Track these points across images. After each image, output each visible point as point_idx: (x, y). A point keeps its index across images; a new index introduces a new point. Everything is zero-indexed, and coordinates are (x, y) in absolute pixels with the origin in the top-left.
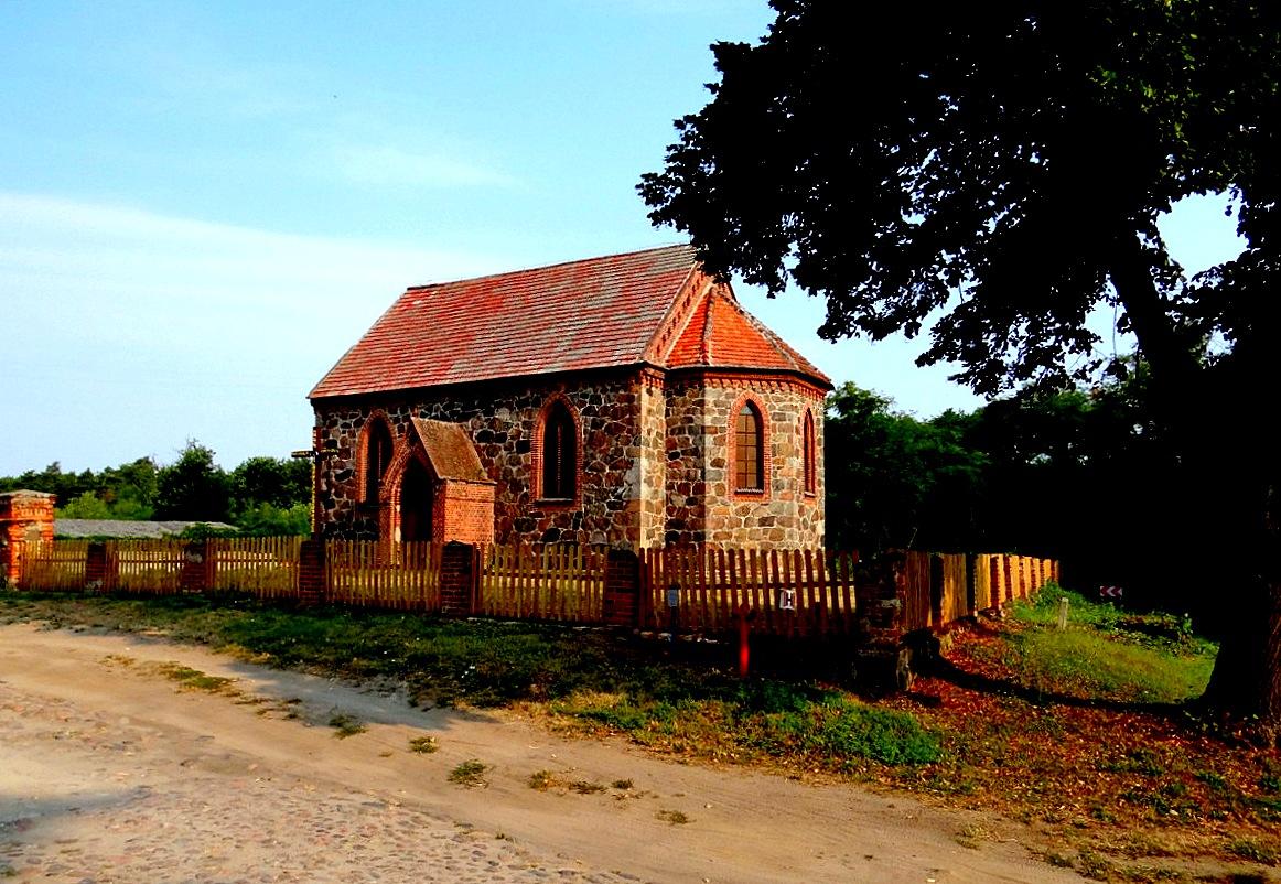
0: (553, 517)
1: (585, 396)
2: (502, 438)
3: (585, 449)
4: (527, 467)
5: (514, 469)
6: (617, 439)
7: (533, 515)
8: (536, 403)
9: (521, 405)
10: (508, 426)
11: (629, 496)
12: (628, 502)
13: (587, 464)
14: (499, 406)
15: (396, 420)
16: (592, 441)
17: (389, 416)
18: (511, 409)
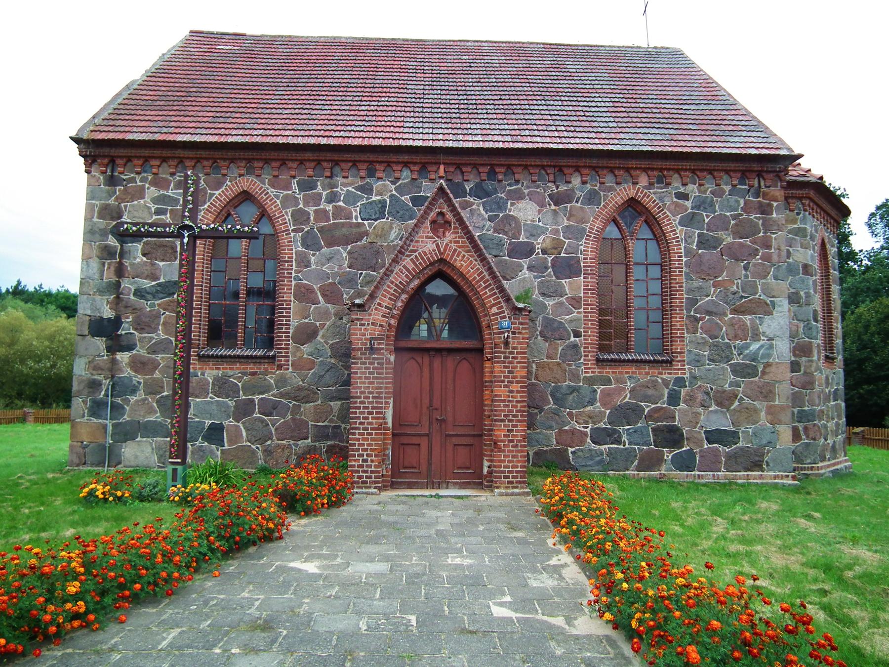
0: (629, 385)
1: (685, 197)
2: (527, 250)
3: (689, 278)
4: (575, 302)
5: (550, 303)
6: (746, 268)
7: (590, 381)
8: (592, 198)
9: (558, 200)
10: (535, 232)
11: (769, 356)
12: (768, 365)
13: (692, 302)
14: (518, 196)
15: (289, 201)
16: (699, 268)
17: (272, 191)
18: (542, 205)
